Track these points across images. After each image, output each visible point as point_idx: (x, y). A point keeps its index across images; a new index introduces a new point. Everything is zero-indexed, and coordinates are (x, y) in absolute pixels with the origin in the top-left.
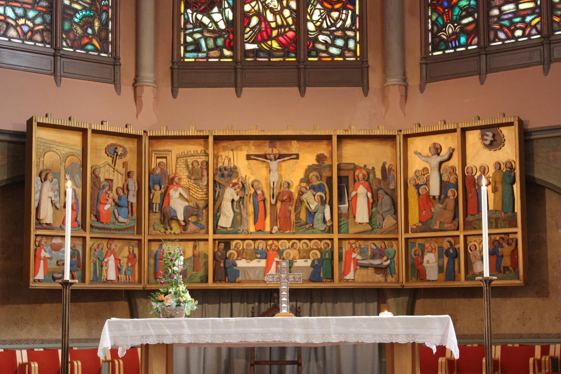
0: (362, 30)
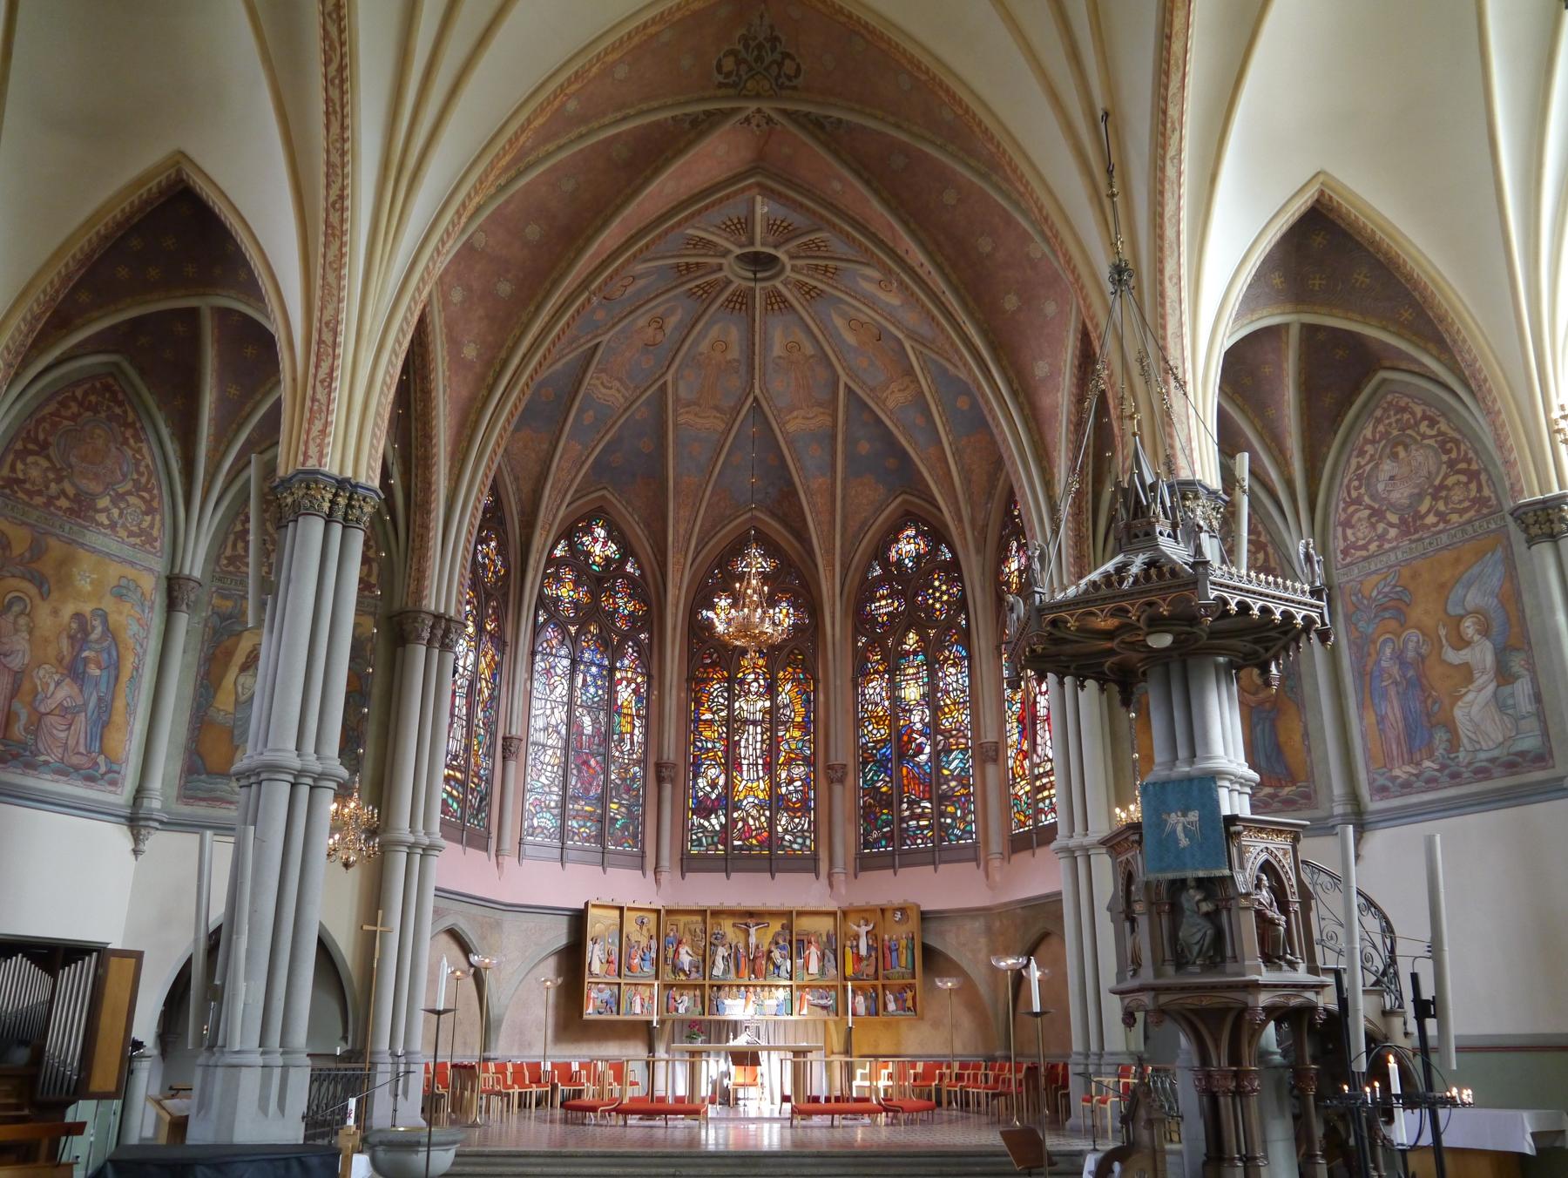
0: (815, 832)
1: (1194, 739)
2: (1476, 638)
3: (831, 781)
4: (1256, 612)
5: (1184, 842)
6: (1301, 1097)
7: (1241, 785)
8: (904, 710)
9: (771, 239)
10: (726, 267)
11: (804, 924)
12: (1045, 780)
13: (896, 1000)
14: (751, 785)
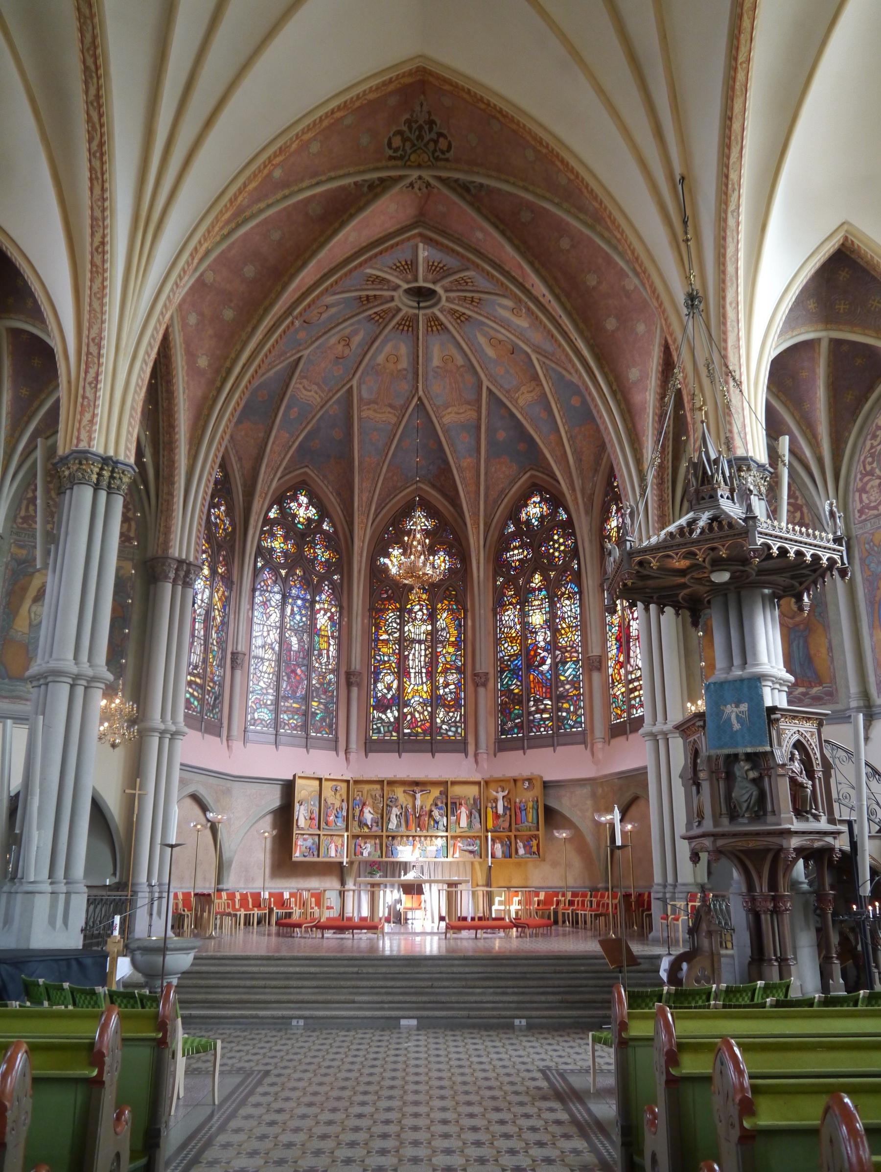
0: (465, 723)
1: (745, 650)
3: (477, 685)
4: (792, 554)
5: (737, 726)
6: (822, 916)
7: (781, 684)
8: (531, 632)
9: (430, 277)
10: (396, 298)
11: (457, 791)
12: (636, 684)
13: (525, 847)
14: (417, 688)
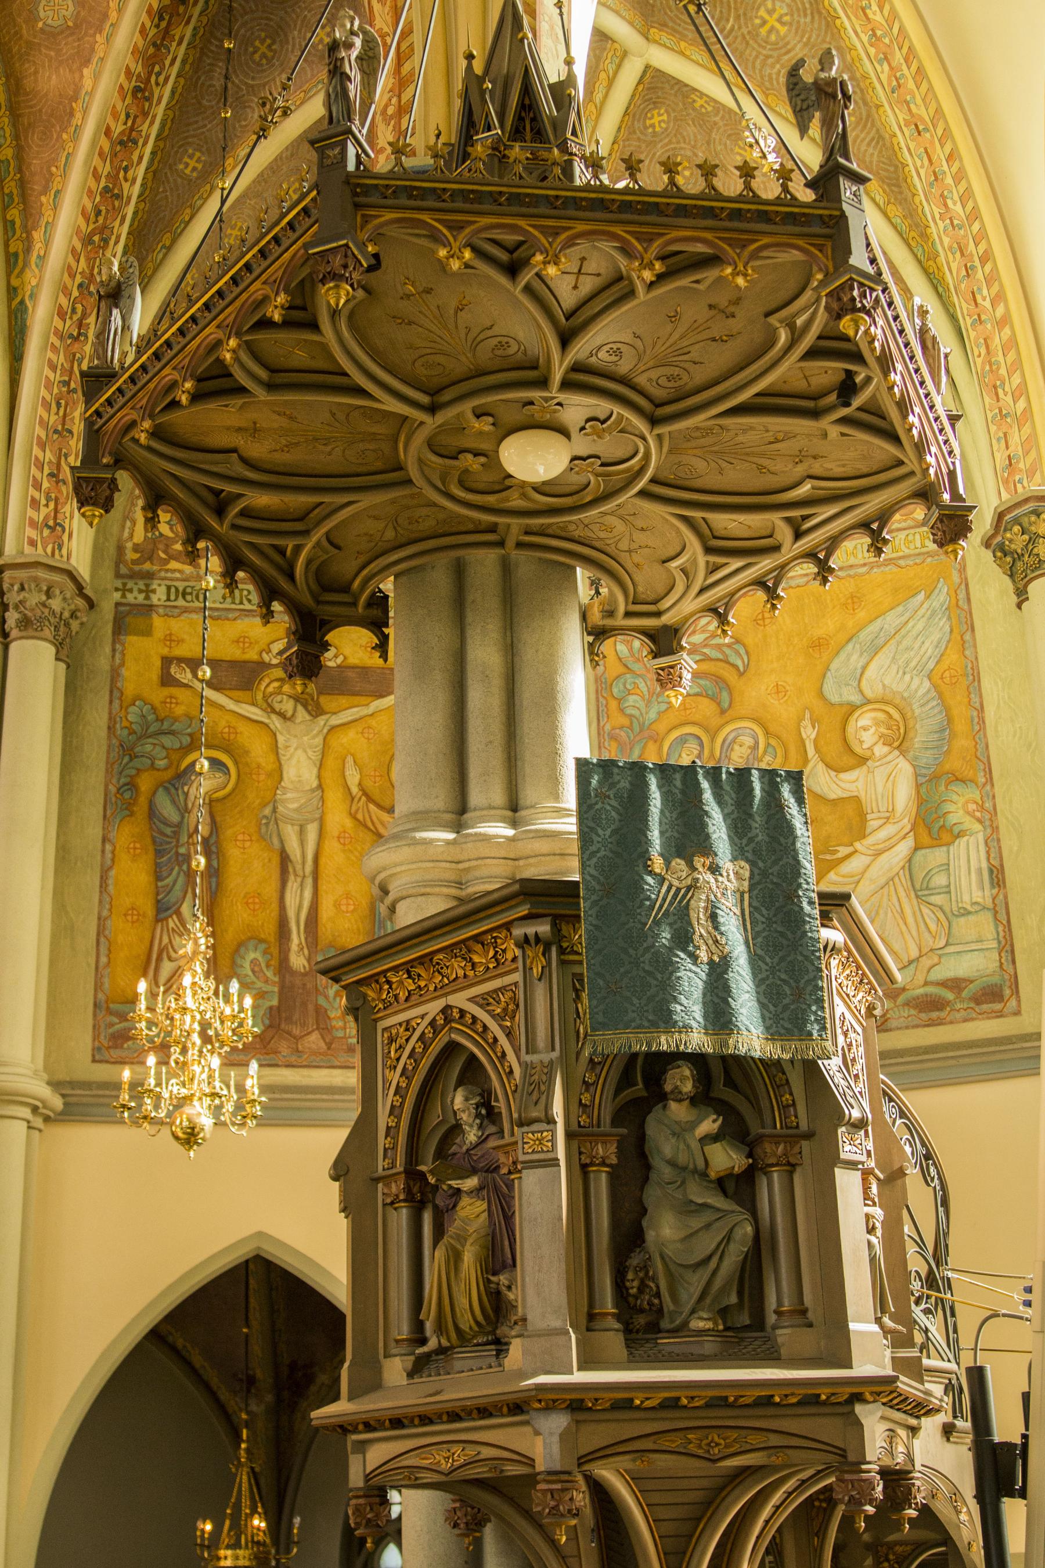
2: (880, 750)
